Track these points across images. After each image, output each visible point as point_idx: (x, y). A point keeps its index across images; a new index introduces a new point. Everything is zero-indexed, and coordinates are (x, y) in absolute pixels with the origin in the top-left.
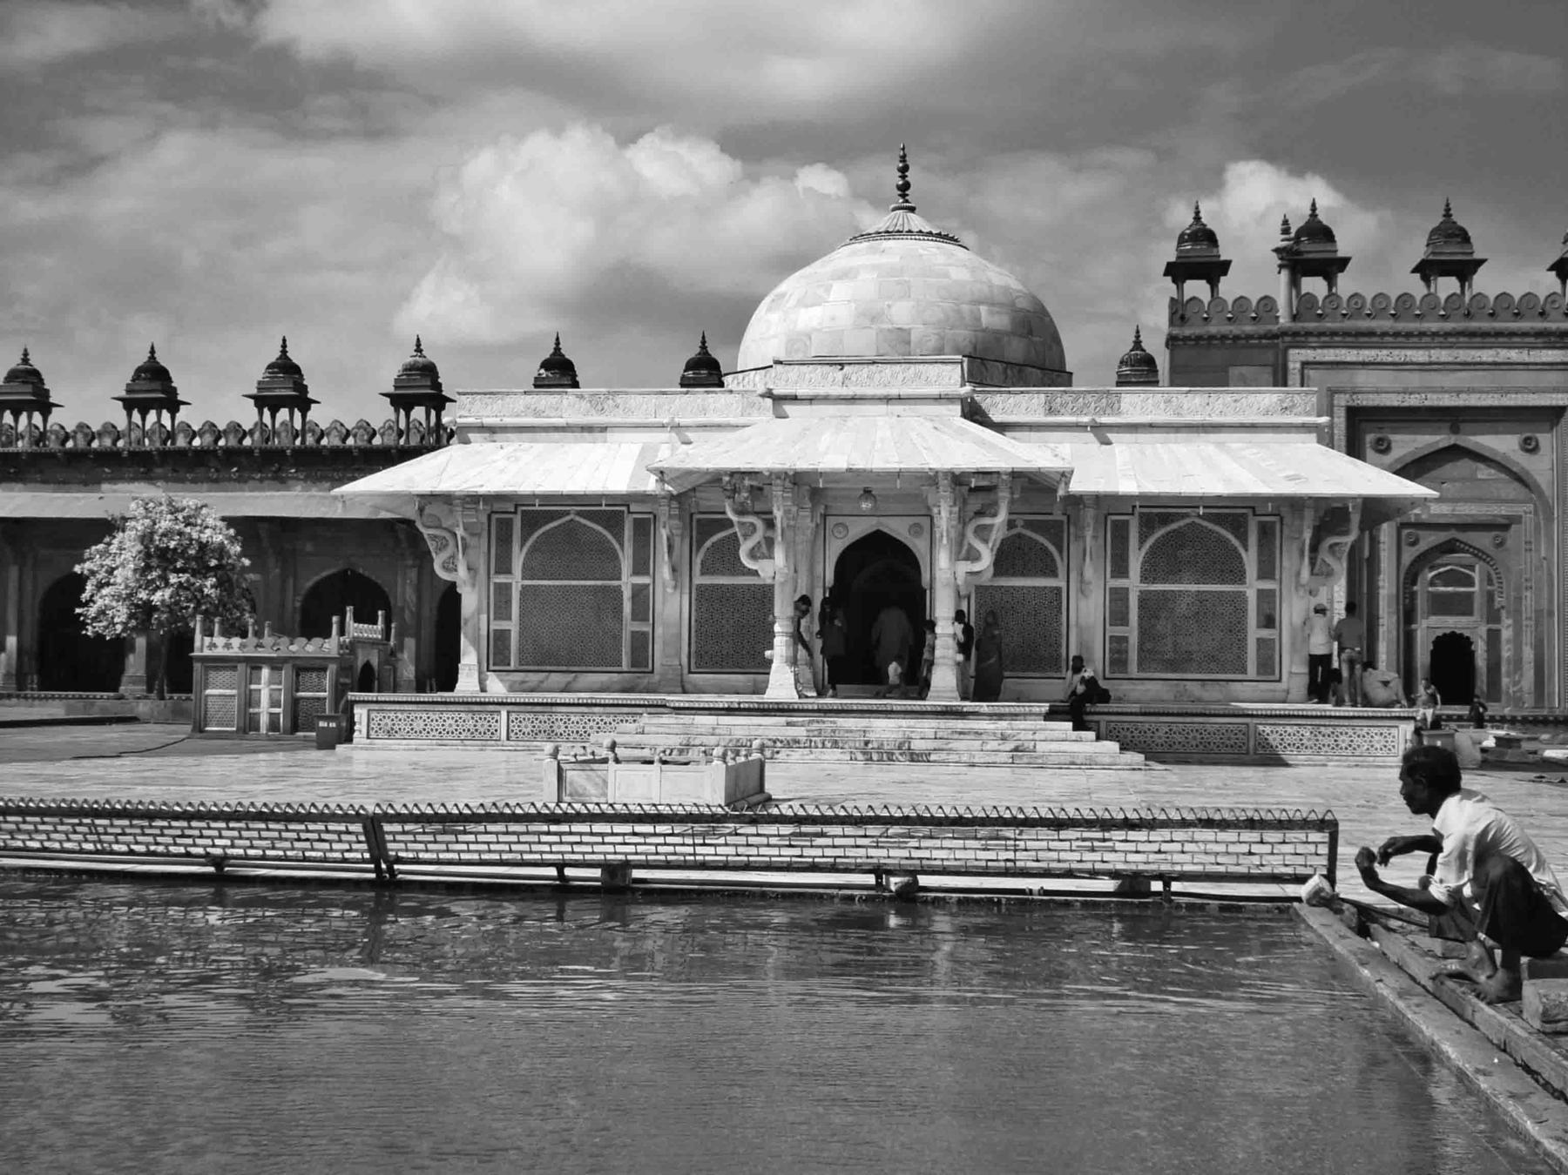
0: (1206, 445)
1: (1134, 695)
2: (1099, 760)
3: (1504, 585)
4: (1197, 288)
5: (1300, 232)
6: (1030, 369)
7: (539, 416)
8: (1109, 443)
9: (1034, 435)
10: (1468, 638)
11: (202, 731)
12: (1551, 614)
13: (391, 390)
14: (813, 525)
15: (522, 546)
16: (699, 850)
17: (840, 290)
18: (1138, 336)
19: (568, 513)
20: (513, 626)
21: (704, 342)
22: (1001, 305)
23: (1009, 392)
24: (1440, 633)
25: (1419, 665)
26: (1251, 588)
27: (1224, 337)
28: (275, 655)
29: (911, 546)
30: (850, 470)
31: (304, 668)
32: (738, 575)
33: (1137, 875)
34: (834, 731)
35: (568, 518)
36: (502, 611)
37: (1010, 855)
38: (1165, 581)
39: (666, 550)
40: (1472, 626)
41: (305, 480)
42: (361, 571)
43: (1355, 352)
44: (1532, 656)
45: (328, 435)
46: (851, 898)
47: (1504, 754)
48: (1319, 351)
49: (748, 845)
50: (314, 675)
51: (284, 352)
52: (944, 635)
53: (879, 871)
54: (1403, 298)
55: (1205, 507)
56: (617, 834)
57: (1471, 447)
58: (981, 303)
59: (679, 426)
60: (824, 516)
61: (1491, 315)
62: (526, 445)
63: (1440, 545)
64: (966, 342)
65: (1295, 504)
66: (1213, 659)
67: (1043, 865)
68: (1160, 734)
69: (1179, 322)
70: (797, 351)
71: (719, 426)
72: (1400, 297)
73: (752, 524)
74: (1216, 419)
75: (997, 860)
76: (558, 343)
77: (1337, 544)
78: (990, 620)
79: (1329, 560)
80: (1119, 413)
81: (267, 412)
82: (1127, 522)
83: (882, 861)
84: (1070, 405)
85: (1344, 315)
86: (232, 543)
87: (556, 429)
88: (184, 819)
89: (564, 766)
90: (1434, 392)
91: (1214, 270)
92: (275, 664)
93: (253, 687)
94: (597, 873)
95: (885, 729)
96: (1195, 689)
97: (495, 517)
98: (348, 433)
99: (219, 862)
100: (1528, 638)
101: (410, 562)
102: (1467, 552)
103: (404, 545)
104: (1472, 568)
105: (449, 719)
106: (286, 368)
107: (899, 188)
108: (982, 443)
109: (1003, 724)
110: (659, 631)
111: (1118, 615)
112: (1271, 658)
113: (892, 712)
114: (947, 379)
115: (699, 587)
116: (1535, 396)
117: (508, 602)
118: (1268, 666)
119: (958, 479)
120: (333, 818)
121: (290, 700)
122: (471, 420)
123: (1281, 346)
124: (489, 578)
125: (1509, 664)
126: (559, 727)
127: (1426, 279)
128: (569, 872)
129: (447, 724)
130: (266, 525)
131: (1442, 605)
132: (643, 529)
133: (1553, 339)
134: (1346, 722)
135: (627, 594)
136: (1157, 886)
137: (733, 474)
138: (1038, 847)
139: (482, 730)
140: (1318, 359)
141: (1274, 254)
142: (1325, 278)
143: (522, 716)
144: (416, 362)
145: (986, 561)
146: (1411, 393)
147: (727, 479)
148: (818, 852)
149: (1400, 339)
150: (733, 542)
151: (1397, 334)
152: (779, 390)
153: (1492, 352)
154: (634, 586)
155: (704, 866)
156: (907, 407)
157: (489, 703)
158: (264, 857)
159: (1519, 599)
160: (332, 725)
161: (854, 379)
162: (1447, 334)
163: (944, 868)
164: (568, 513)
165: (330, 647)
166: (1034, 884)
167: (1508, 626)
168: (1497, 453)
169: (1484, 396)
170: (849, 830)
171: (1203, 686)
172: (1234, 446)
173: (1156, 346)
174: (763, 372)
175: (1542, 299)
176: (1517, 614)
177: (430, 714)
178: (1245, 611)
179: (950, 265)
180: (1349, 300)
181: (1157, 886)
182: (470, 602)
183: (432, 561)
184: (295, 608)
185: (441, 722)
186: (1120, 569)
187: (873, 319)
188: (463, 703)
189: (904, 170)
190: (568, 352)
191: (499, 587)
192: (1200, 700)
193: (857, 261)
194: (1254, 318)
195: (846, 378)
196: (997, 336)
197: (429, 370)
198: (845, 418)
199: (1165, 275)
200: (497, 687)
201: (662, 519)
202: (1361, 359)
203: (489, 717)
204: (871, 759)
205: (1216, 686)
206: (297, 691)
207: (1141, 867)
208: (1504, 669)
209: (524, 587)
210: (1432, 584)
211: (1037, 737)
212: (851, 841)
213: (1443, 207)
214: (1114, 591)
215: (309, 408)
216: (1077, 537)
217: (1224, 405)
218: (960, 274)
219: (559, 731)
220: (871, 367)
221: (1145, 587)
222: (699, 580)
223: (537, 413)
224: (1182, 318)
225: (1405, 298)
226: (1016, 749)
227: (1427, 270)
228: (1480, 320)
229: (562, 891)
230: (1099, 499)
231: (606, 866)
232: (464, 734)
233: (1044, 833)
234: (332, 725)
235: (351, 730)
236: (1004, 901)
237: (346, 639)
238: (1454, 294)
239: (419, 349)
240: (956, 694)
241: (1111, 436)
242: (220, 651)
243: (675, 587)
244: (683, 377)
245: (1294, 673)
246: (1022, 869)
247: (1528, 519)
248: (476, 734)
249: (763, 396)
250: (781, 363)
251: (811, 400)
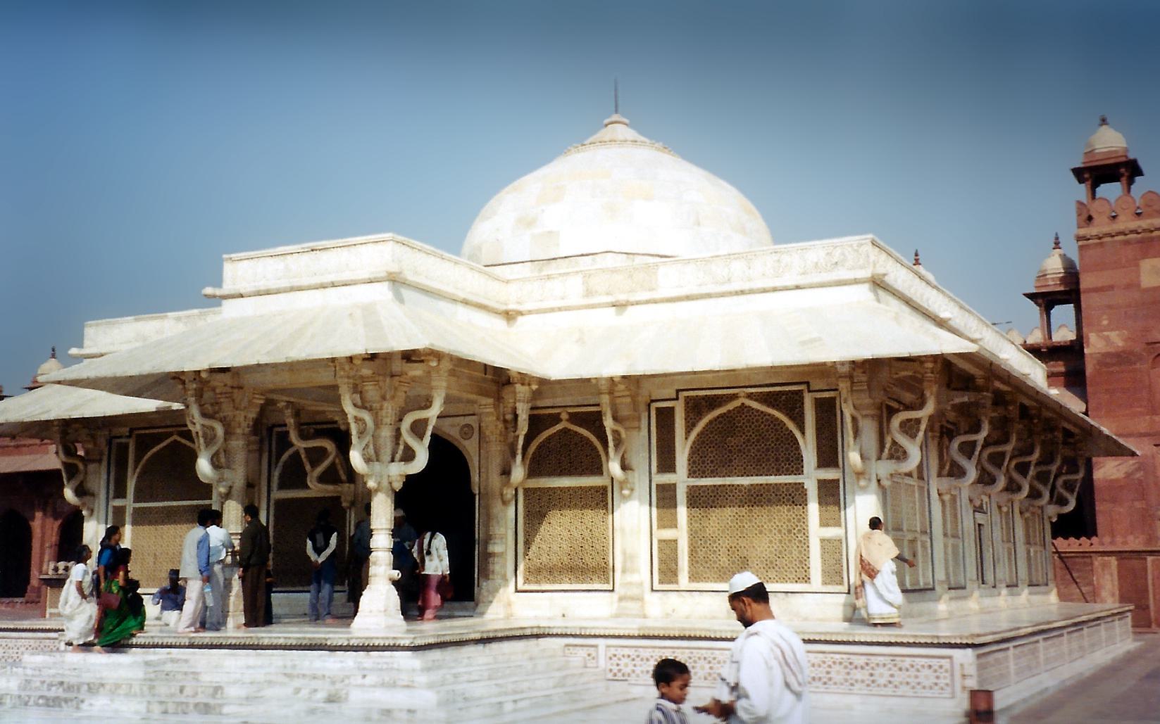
4: (1110, 191)
26: (811, 476)
38: (714, 474)
77: (909, 420)
79: (903, 440)
82: (672, 409)
186: (667, 464)
214: (661, 488)
222: (278, 495)
224: (1090, 218)
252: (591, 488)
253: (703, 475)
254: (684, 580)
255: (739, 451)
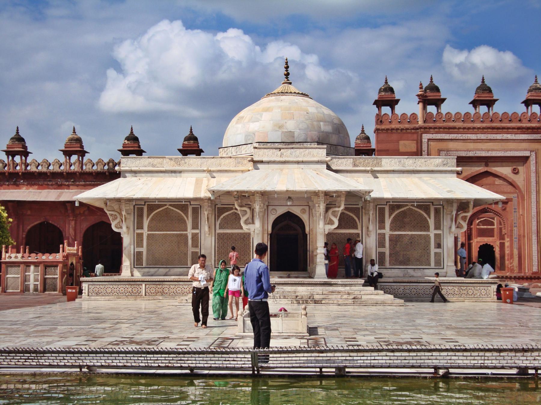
0: (415, 178)
1: (387, 275)
2: (386, 302)
3: (506, 225)
4: (386, 110)
5: (427, 88)
6: (340, 147)
7: (154, 167)
8: (378, 178)
9: (349, 174)
10: (492, 246)
11: (5, 292)
12: (524, 236)
13: (63, 148)
14: (264, 209)
15: (148, 217)
16: (372, 361)
17: (266, 116)
18: (363, 129)
19: (166, 205)
20: (144, 250)
21: (191, 130)
22: (328, 122)
23: (339, 158)
24: (482, 244)
25: (474, 256)
26: (432, 233)
27: (397, 129)
28: (36, 261)
29: (301, 217)
30: (287, 191)
31: (48, 266)
32: (233, 229)
33: (527, 368)
34: (283, 292)
36: (139, 243)
37: (482, 362)
38: (399, 230)
39: (206, 220)
40: (494, 241)
41: (27, 185)
42: (50, 222)
43: (448, 135)
44: (517, 253)
45: (30, 165)
46: (426, 378)
47: (523, 294)
48: (434, 135)
49: (390, 359)
50: (52, 268)
51: (18, 132)
52: (321, 253)
53: (436, 368)
54: (467, 114)
55: (417, 202)
56: (343, 356)
57: (494, 172)
58: (321, 121)
59: (210, 171)
60: (268, 206)
61: (501, 121)
62: (150, 178)
63: (481, 210)
64: (316, 136)
65: (449, 202)
66: (418, 260)
67: (494, 365)
68: (401, 290)
69: (379, 123)
70: (249, 139)
71: (226, 171)
72: (465, 114)
73: (246, 211)
74: (419, 168)
75: (478, 363)
76: (132, 130)
78: (334, 247)
79: (462, 222)
80: (381, 166)
81: (10, 158)
82: (384, 208)
83: (437, 364)
84: (362, 163)
85: (444, 121)
86: (4, 212)
87: (161, 172)
88: (182, 354)
89: (245, 319)
90: (478, 151)
91: (392, 103)
92: (36, 264)
93: (27, 274)
94: (334, 370)
95: (303, 291)
96: (411, 272)
97: (136, 206)
98: (39, 164)
99: (191, 369)
100: (516, 245)
101: (71, 218)
102: (491, 212)
103: (69, 212)
104: (493, 219)
105: (122, 288)
106: (19, 139)
107: (285, 75)
108: (337, 180)
109: (348, 288)
111: (381, 243)
112: (440, 260)
113: (304, 284)
114: (320, 155)
115: (218, 234)
116: (518, 152)
117: (142, 240)
118: (439, 263)
119: (327, 194)
120: (240, 352)
121: (42, 278)
122: (127, 168)
123: (420, 133)
124: (134, 231)
125: (508, 255)
126: (166, 290)
127: (475, 107)
128: (323, 370)
129: (120, 290)
130: (10, 204)
131: (482, 233)
132: (196, 212)
133: (524, 130)
134: (471, 285)
135: (190, 237)
136: (533, 372)
137: (237, 192)
138: (491, 359)
139: (135, 292)
140: (434, 138)
141: (417, 97)
142: (436, 106)
143: (151, 286)
144: (73, 137)
145: (336, 224)
146: (470, 151)
147: (236, 193)
148: (415, 361)
149: (465, 130)
150: (237, 217)
151: (464, 128)
152: (256, 159)
153: (501, 135)
154: (192, 234)
155: (373, 367)
156: (306, 165)
157: (138, 281)
158: (211, 367)
159: (512, 231)
160: (74, 291)
161: (285, 154)
162: (484, 128)
163: (458, 366)
164: (166, 205)
165: (59, 257)
166: (489, 371)
167: (508, 241)
168: (502, 174)
169: (498, 152)
170: (427, 354)
171: (414, 271)
172: (425, 179)
173: (370, 132)
174: (235, 148)
175: (520, 116)
176: (511, 236)
177: (114, 287)
178: (429, 242)
179: (308, 106)
180: (446, 114)
181: (533, 372)
182: (127, 240)
183: (110, 225)
184: (23, 237)
185: (118, 288)
186: (382, 227)
187: (280, 127)
188: (127, 281)
189: (287, 68)
190: (136, 134)
191: (138, 234)
192: (413, 276)
193: (272, 104)
194: (409, 122)
195: (282, 154)
196: (327, 134)
197: (79, 141)
198: (282, 170)
199: (374, 104)
200: (137, 275)
201: (206, 207)
202: (450, 138)
203: (137, 287)
204: (299, 303)
205: (419, 271)
206: (46, 275)
207: (528, 365)
208: (506, 258)
209: (148, 234)
210: (478, 225)
211: (361, 293)
212: (427, 358)
213: (482, 79)
214: (379, 234)
215: (28, 156)
216: (365, 214)
217: (421, 163)
218: (312, 110)
219: (166, 292)
220: (292, 150)
221: (392, 233)
222: (219, 231)
223: (153, 166)
224: (381, 121)
225: (467, 114)
226: (354, 298)
227: (475, 103)
228: (496, 123)
229: (321, 377)
230: (375, 200)
231: (337, 368)
233: (495, 354)
234: (74, 291)
235: (81, 292)
236: (480, 377)
237: (65, 254)
238: (486, 113)
239: (74, 132)
240: (326, 276)
241: (378, 175)
242: (13, 260)
243: (209, 234)
244: (183, 144)
245: (449, 266)
246: (486, 366)
247: (515, 200)
249: (249, 161)
250: (256, 148)
251: (269, 162)
252: (353, 234)
253: (395, 230)
254: (387, 264)
255: (408, 223)
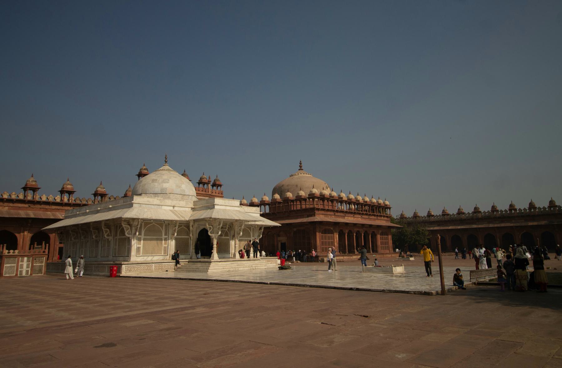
19: (153, 223)
20: (141, 246)
35: (153, 224)
110: (169, 247)
157: (150, 263)
164: (153, 223)
183: (125, 232)
223: (149, 202)
232: (145, 270)
248: (148, 270)
